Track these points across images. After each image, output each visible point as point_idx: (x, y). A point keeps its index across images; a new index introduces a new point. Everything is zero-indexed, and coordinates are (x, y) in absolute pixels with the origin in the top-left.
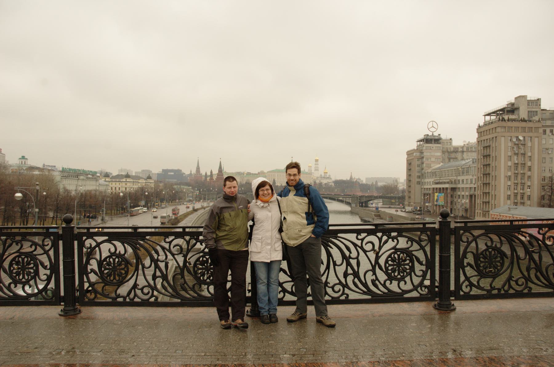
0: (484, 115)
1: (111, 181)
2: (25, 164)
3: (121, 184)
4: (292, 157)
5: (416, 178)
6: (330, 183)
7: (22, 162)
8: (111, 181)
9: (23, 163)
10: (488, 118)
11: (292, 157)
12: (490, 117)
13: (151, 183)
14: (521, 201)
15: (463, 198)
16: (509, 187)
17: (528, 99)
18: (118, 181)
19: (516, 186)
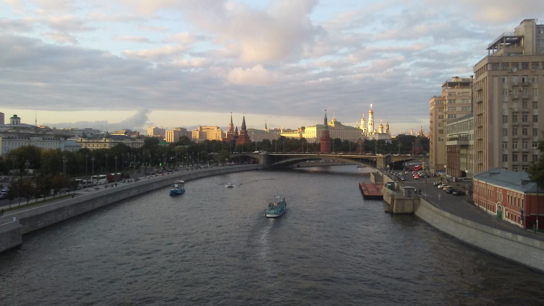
0: (488, 49)
1: (88, 142)
2: (17, 124)
3: (99, 145)
4: (326, 110)
5: (438, 133)
6: (386, 139)
7: (13, 121)
8: (88, 142)
9: (15, 123)
10: (491, 51)
11: (326, 110)
12: (493, 51)
13: (140, 143)
14: (524, 163)
15: (471, 158)
16: (505, 144)
17: (538, 23)
18: (96, 142)
19: (526, 142)
